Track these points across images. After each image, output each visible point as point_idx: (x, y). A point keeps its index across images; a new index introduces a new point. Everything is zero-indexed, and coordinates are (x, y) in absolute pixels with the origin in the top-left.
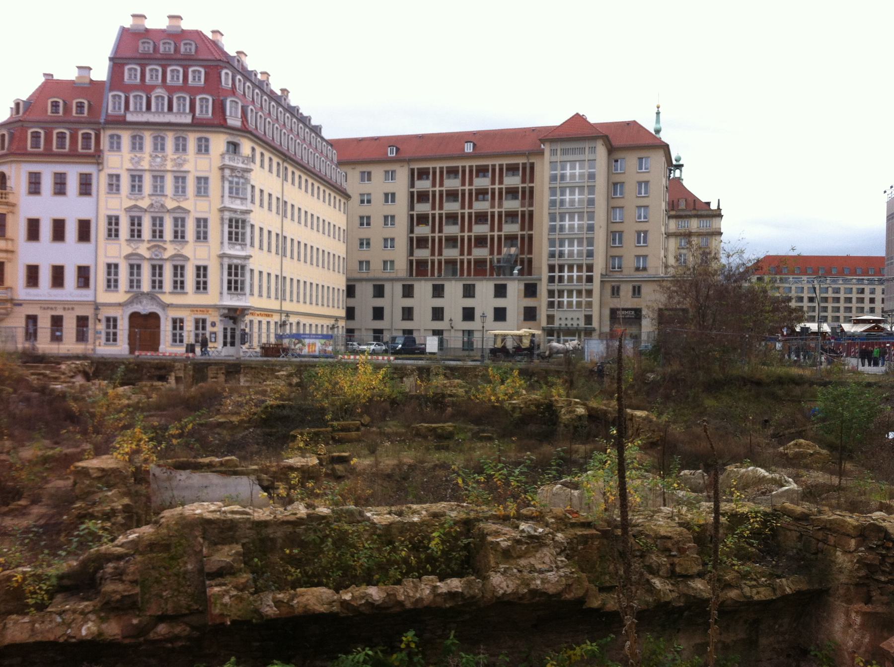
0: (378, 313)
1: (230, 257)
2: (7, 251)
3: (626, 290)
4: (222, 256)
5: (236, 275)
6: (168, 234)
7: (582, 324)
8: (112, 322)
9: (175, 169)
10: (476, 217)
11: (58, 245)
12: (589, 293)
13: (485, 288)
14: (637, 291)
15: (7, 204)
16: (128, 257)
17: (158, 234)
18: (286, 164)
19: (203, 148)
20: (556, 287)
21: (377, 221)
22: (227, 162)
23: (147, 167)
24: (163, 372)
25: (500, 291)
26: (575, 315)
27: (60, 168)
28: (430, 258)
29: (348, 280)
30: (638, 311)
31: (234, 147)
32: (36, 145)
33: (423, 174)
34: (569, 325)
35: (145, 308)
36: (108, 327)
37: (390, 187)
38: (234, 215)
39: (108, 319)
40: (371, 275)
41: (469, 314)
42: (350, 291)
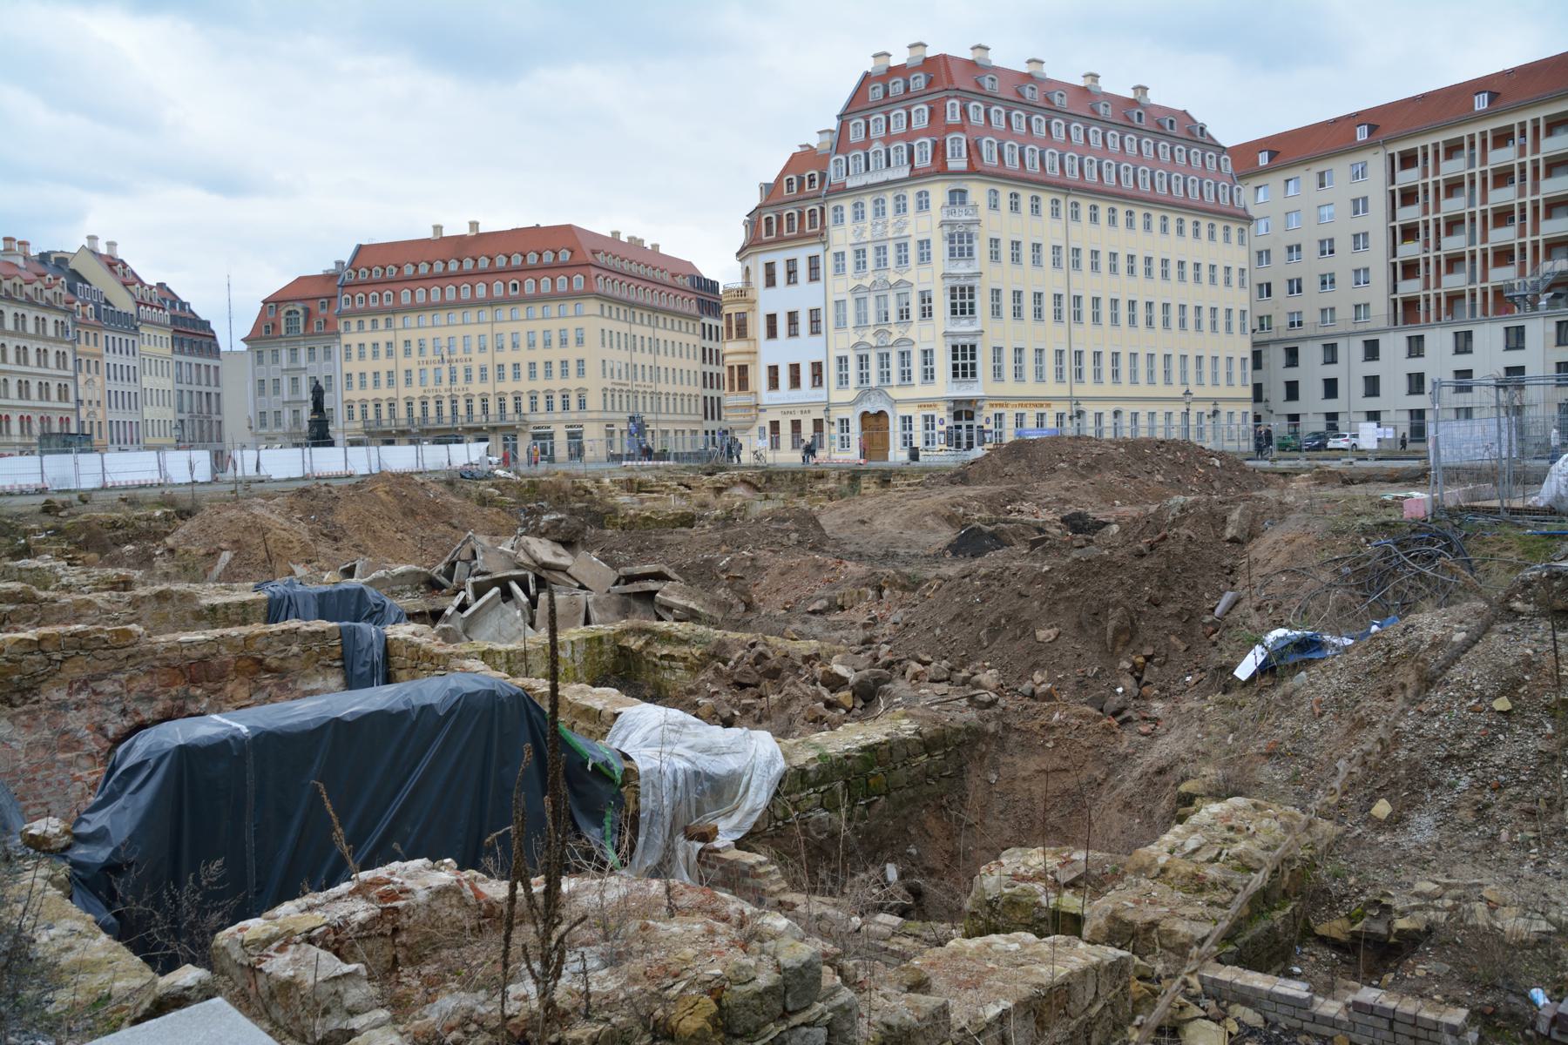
0: (1331, 388)
1: (953, 335)
4: (946, 334)
6: (893, 317)
8: (844, 422)
13: (1489, 336)
16: (855, 346)
18: (1071, 199)
19: (923, 205)
27: (790, 254)
28: (1421, 294)
29: (1255, 344)
31: (958, 197)
32: (769, 233)
33: (1408, 160)
37: (1359, 190)
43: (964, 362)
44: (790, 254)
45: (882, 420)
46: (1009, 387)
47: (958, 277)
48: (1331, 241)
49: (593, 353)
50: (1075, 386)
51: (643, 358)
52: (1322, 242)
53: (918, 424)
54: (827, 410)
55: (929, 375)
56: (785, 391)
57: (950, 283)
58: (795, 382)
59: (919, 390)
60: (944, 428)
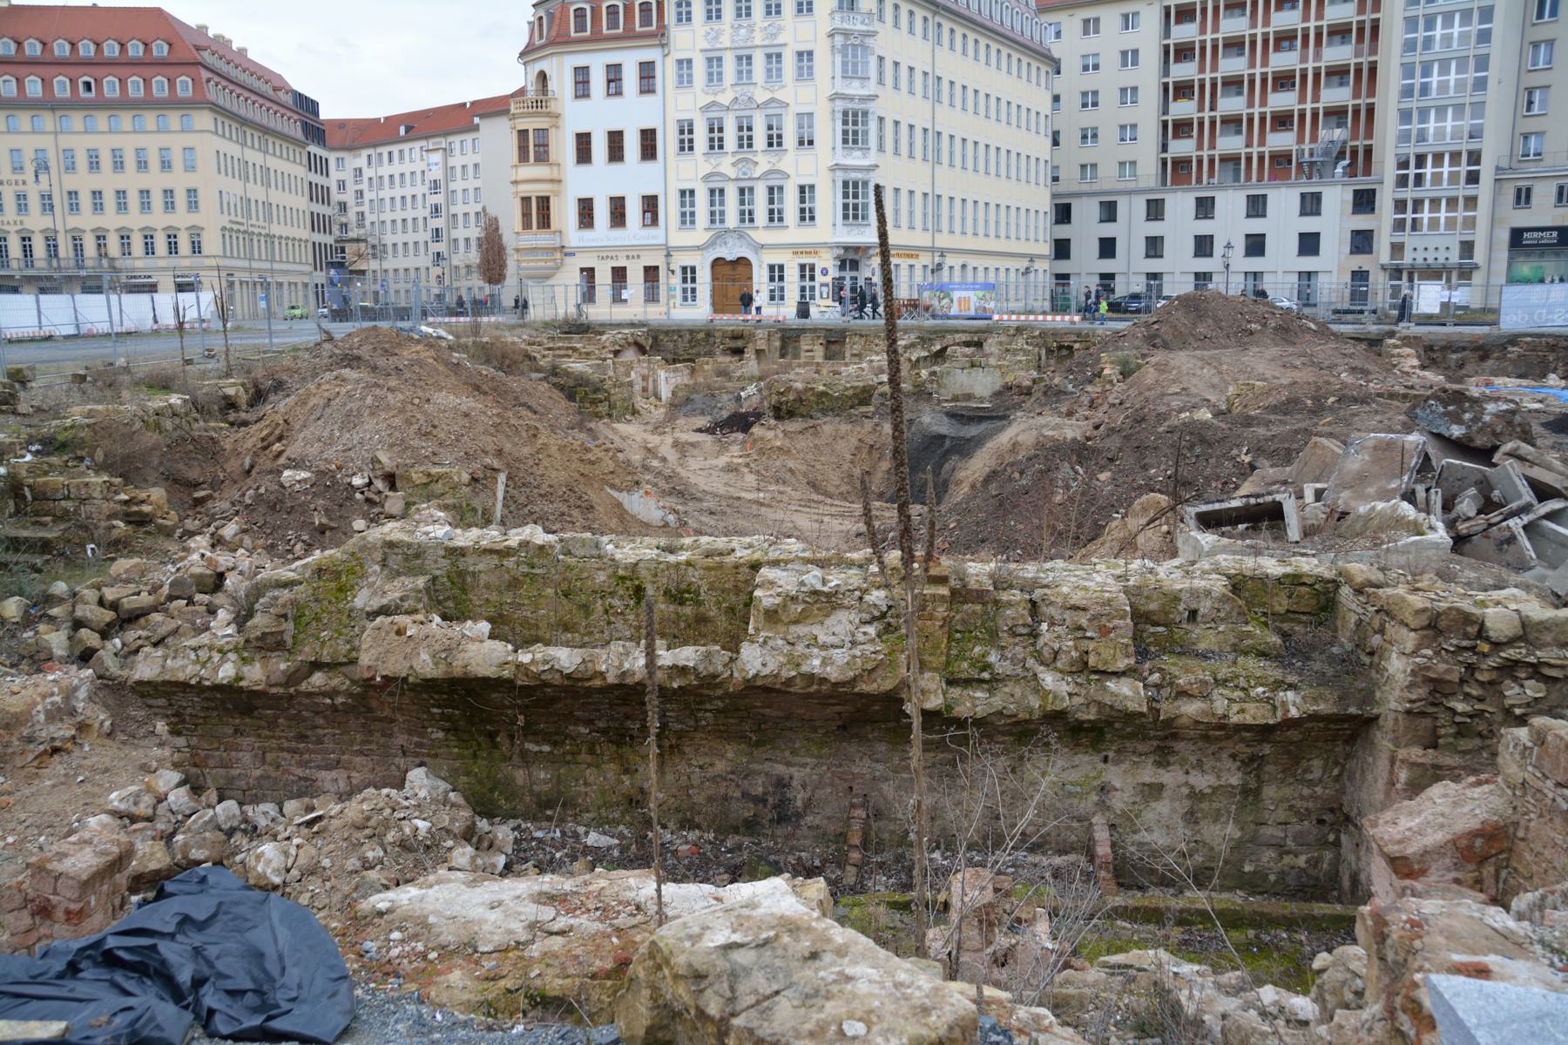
1: (846, 169)
2: (552, 181)
4: (836, 168)
5: (856, 196)
7: (1455, 258)
8: (689, 273)
9: (766, 42)
10: (1274, 79)
11: (616, 167)
12: (1471, 202)
13: (1284, 200)
15: (549, 115)
16: (706, 178)
17: (745, 142)
18: (938, 19)
20: (1409, 193)
21: (1109, 98)
22: (838, 24)
23: (728, 44)
24: (739, 343)
25: (1311, 204)
26: (1441, 243)
27: (613, 58)
28: (1194, 154)
32: (581, 27)
33: (1185, 14)
34: (1430, 261)
35: (730, 252)
36: (685, 280)
37: (1129, 40)
38: (850, 105)
39: (684, 269)
42: (1063, 214)
43: (859, 197)
44: (613, 58)
45: (740, 269)
47: (851, 98)
48: (1095, 93)
49: (210, 182)
51: (256, 192)
52: (1084, 94)
53: (792, 274)
54: (668, 255)
55: (806, 216)
57: (840, 105)
59: (793, 232)
60: (828, 279)
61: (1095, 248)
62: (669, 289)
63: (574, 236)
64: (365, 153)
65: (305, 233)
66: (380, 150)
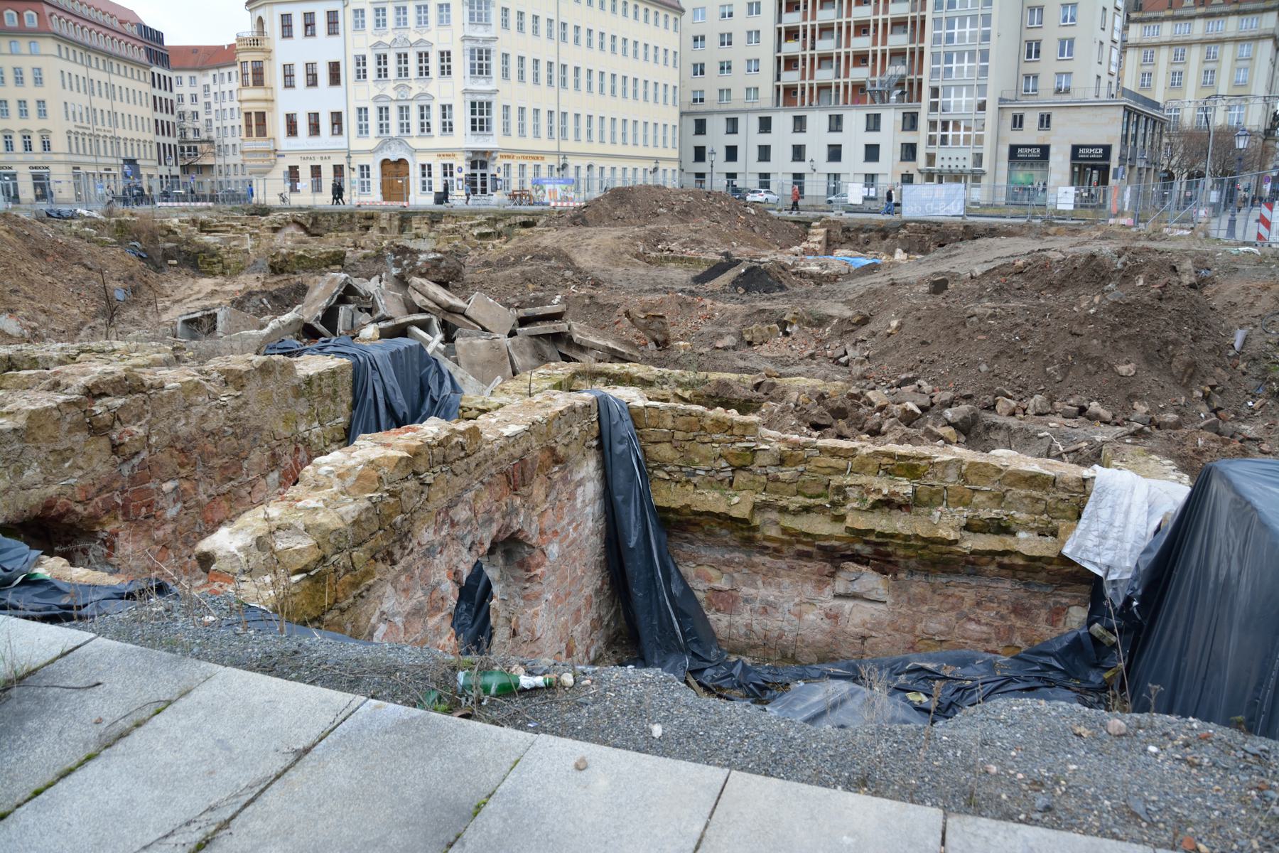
1: (472, 92)
2: (266, 100)
3: (1032, 119)
4: (466, 92)
5: (481, 113)
8: (365, 170)
10: (856, 27)
13: (854, 118)
14: (1045, 121)
15: (262, 50)
16: (376, 99)
21: (739, 38)
25: (874, 123)
26: (961, 154)
30: (1045, 151)
34: (953, 167)
36: (362, 176)
38: (476, 45)
39: (362, 167)
40: (757, 106)
41: (798, 153)
43: (480, 118)
45: (401, 167)
46: (514, 142)
47: (477, 40)
48: (730, 35)
50: (562, 143)
51: (102, 103)
52: (722, 35)
53: (437, 172)
54: (349, 157)
55: (447, 127)
56: (303, 137)
57: (468, 45)
58: (315, 129)
59: (438, 140)
60: (462, 175)
61: (789, 153)
62: (351, 182)
63: (284, 143)
64: (211, 73)
65: (150, 135)
66: (222, 71)
